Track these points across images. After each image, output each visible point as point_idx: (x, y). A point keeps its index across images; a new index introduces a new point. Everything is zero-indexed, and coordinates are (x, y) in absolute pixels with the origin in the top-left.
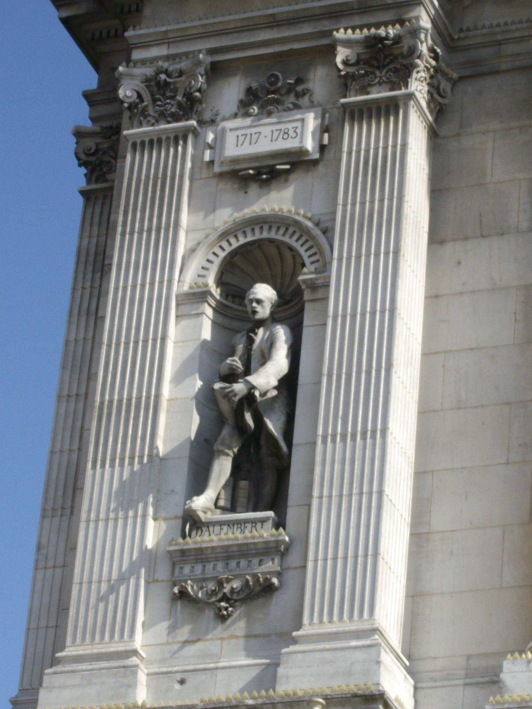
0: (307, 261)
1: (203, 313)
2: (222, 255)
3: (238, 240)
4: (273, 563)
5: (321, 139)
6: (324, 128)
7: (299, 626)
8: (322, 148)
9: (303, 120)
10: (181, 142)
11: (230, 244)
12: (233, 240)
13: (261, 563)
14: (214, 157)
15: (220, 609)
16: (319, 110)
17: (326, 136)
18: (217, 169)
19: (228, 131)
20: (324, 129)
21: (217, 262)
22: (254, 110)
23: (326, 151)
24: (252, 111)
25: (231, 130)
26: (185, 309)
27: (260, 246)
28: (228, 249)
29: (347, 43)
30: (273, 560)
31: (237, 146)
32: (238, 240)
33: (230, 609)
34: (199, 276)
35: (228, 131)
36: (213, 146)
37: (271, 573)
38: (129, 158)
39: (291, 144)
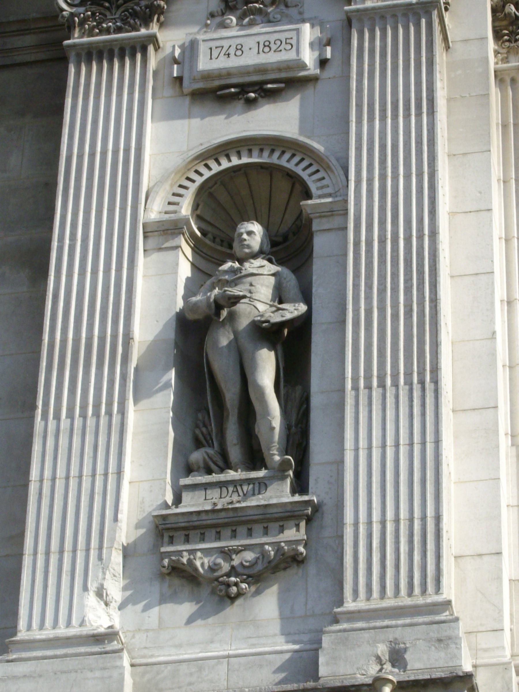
0: (313, 188)
1: (178, 247)
2: (199, 180)
3: (219, 164)
4: (298, 530)
7: (341, 602)
9: (298, 30)
10: (139, 56)
11: (210, 169)
12: (212, 164)
13: (282, 530)
14: (183, 72)
15: (228, 585)
17: (329, 49)
18: (188, 86)
19: (201, 43)
21: (193, 187)
22: (232, 20)
23: (328, 66)
24: (228, 21)
25: (204, 41)
26: (152, 242)
27: (246, 174)
28: (207, 174)
30: (298, 526)
31: (211, 59)
32: (219, 164)
33: (244, 586)
34: (169, 203)
36: (180, 60)
37: (297, 542)
38: (72, 70)
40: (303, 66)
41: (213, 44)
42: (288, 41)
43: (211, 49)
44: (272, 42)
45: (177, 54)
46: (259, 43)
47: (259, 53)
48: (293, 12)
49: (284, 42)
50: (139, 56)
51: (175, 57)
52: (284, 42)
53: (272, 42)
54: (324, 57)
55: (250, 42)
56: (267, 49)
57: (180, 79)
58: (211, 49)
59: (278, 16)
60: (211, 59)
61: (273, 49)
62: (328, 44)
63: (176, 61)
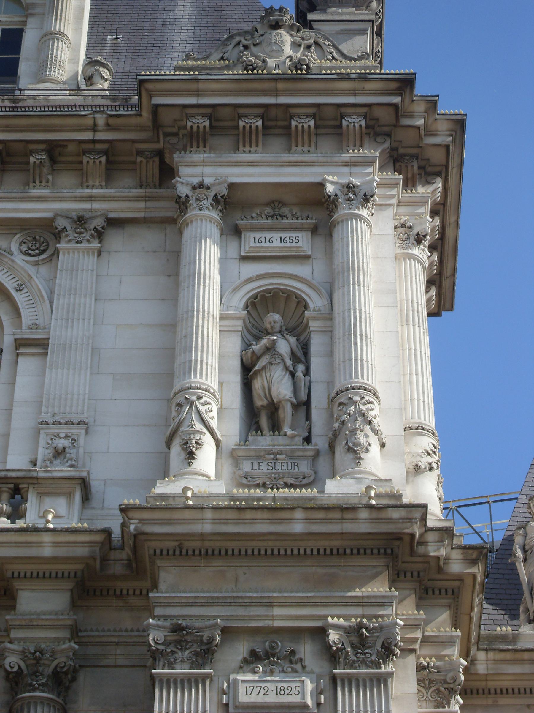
5: (318, 698)
6: (319, 690)
8: (319, 704)
10: (200, 686)
14: (229, 701)
16: (314, 676)
19: (240, 682)
20: (318, 692)
25: (243, 681)
29: (336, 627)
31: (247, 694)
35: (240, 682)
36: (227, 692)
39: (295, 699)
40: (305, 706)
41: (248, 685)
42: (297, 688)
43: (247, 687)
44: (286, 688)
45: (225, 688)
46: (277, 687)
47: (277, 694)
48: (298, 667)
49: (293, 689)
50: (200, 686)
51: (223, 689)
52: (293, 689)
53: (286, 688)
54: (319, 702)
55: (272, 687)
56: (282, 692)
57: (227, 705)
58: (247, 687)
59: (290, 669)
60: (247, 694)
61: (286, 694)
62: (321, 693)
63: (225, 694)
